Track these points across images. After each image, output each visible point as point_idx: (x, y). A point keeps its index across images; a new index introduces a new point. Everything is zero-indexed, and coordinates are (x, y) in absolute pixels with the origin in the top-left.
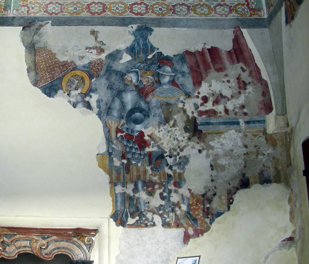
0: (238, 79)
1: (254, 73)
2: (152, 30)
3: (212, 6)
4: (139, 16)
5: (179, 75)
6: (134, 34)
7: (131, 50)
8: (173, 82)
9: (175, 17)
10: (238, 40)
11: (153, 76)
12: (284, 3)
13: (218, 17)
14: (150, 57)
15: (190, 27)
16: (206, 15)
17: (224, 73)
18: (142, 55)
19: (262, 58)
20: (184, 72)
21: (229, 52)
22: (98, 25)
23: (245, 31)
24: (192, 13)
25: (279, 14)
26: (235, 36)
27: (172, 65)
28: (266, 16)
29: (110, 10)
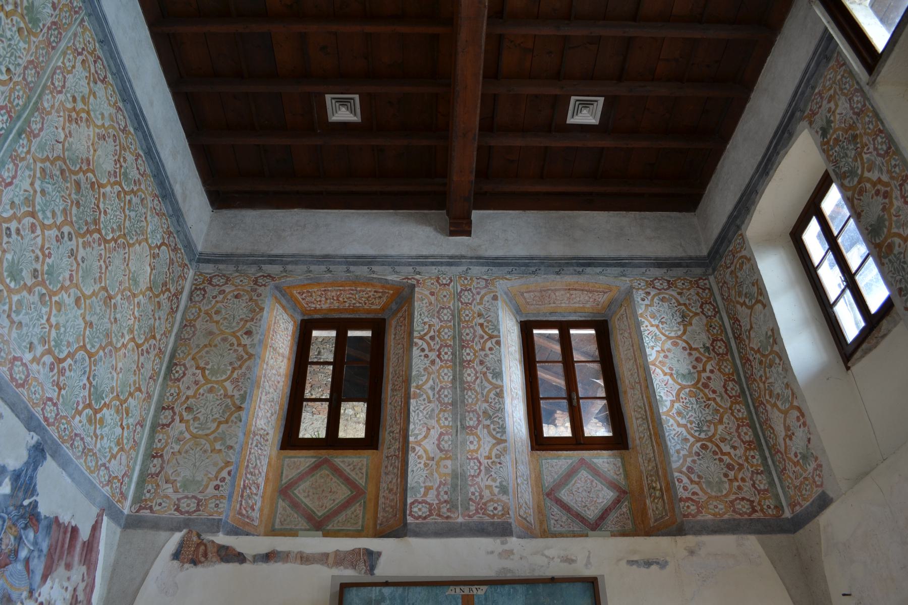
0: (75, 590)
1: (88, 589)
2: (45, 458)
3: (100, 462)
4: (45, 424)
5: (36, 554)
6: (29, 450)
7: (17, 476)
8: (27, 561)
9: (70, 453)
10: (96, 528)
11: (15, 538)
12: (185, 531)
13: (96, 482)
14: (26, 503)
15: (73, 480)
16: (92, 472)
17: (67, 574)
18: (21, 494)
19: (104, 569)
20: (42, 551)
21: (84, 543)
22: (8, 405)
23: (105, 518)
24: (82, 461)
25: (163, 534)
26: (96, 522)
27: (36, 532)
28: (126, 511)
29: (29, 389)
